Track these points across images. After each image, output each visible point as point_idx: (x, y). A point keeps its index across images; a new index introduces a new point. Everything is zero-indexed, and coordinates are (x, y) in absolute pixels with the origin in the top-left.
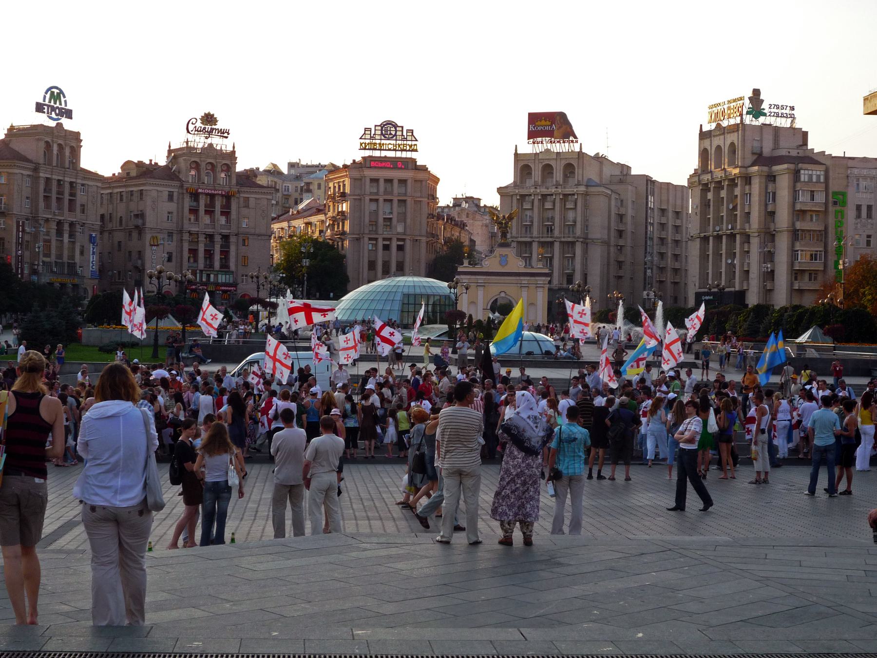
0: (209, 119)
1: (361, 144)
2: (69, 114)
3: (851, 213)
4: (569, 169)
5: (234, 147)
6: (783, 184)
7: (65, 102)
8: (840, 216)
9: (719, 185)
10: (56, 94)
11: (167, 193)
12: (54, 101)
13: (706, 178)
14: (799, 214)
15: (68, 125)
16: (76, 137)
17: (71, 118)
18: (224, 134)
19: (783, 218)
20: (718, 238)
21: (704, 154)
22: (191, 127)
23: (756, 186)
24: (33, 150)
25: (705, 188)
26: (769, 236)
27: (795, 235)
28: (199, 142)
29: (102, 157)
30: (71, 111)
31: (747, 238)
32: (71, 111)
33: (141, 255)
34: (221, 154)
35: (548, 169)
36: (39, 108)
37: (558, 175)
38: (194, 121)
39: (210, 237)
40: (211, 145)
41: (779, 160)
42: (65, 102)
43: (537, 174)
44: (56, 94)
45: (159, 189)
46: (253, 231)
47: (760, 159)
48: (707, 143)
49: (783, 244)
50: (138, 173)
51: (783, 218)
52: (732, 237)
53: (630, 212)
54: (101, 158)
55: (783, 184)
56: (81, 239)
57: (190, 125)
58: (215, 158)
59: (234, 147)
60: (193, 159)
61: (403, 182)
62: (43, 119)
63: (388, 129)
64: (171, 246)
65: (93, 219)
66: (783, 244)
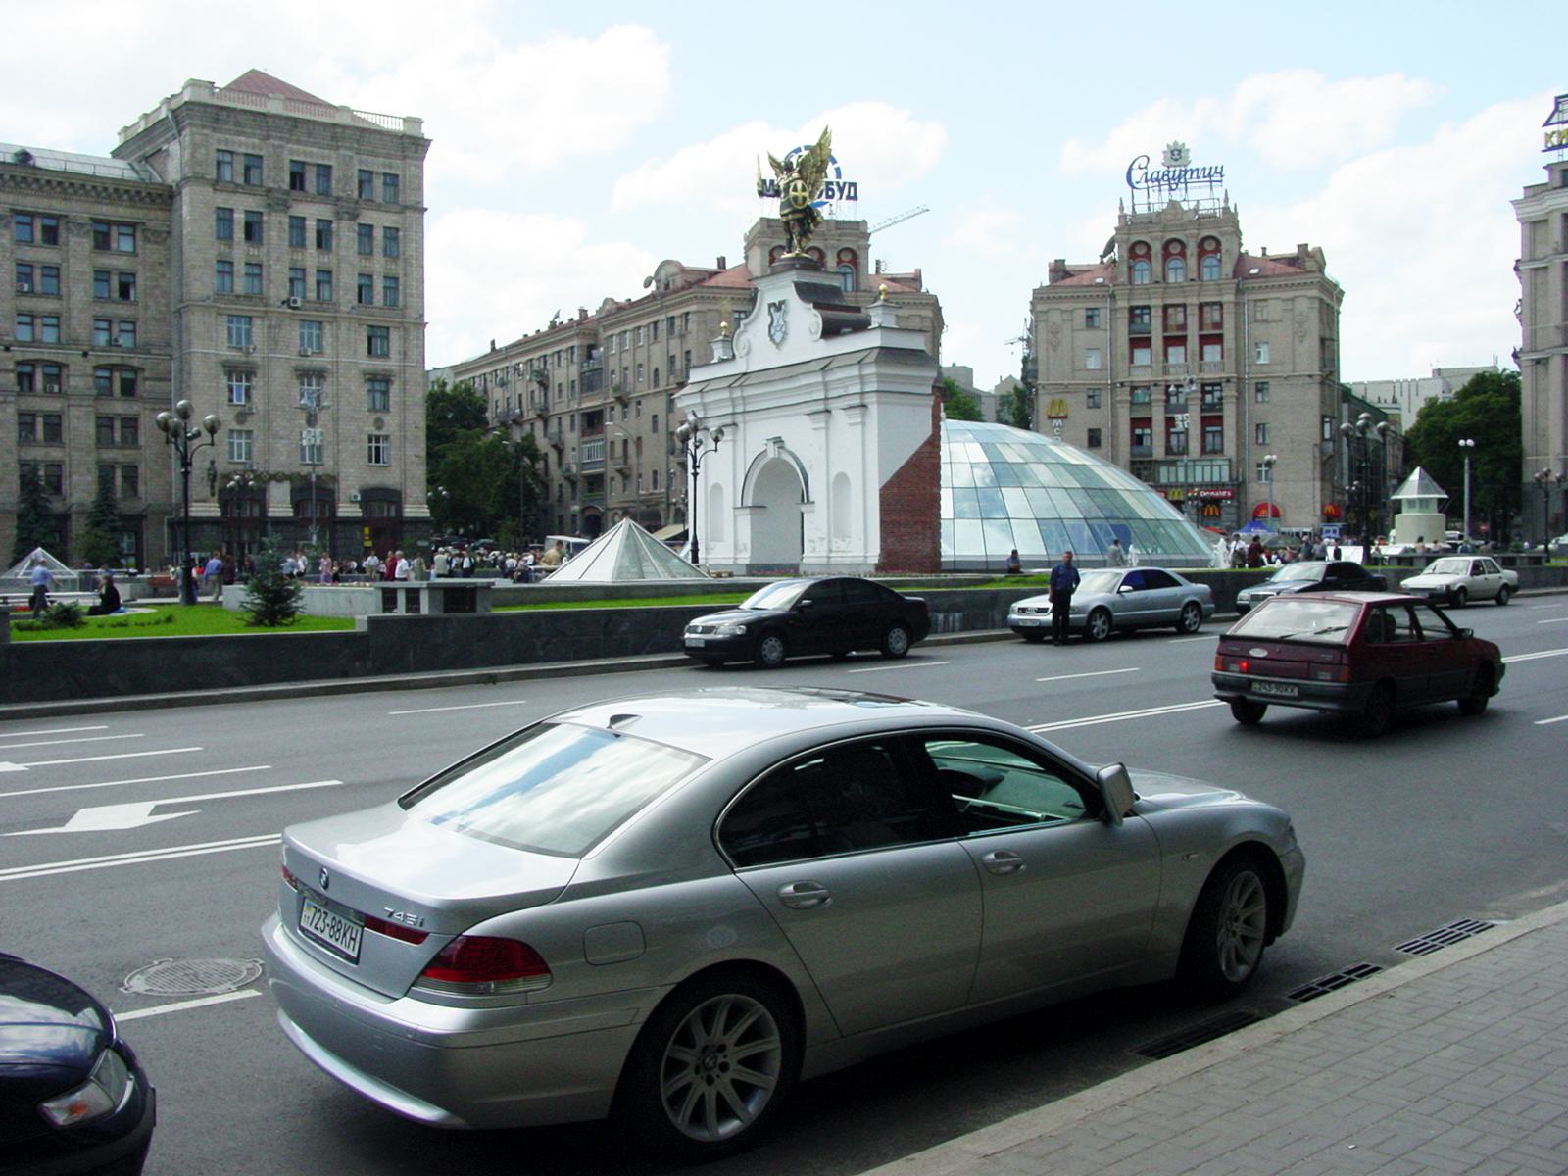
0: (1176, 153)
1: (1549, 137)
2: (850, 191)
5: (1226, 200)
7: (838, 170)
11: (1083, 313)
16: (858, 231)
17: (855, 198)
18: (1213, 176)
22: (1137, 175)
28: (1157, 200)
30: (854, 185)
32: (854, 185)
34: (1201, 220)
38: (1143, 162)
40: (1173, 204)
42: (838, 170)
45: (1063, 306)
46: (1277, 370)
57: (1133, 172)
58: (1183, 228)
59: (1226, 200)
60: (1135, 239)
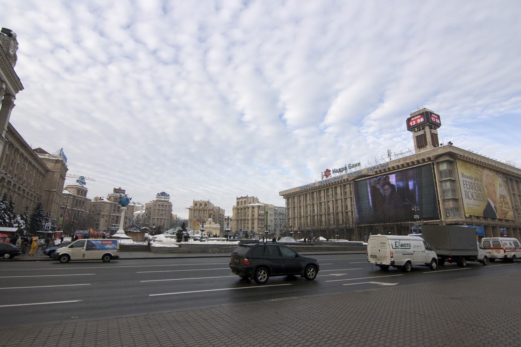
2: (85, 183)
3: (269, 215)
4: (206, 205)
8: (267, 216)
9: (242, 209)
12: (82, 180)
13: (238, 207)
14: (259, 215)
15: (84, 186)
19: (256, 216)
20: (241, 220)
21: (238, 203)
25: (238, 209)
27: (259, 219)
29: (91, 196)
31: (248, 220)
33: (98, 220)
35: (201, 205)
36: (78, 181)
37: (203, 206)
48: (238, 200)
49: (256, 222)
51: (256, 216)
52: (245, 220)
61: (166, 206)
63: (163, 194)
66: (256, 222)
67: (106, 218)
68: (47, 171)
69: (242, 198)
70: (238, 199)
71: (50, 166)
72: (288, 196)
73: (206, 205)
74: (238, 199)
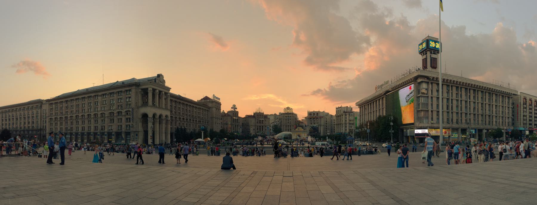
6: (348, 116)
10: (234, 106)
12: (234, 107)
14: (350, 120)
19: (348, 121)
23: (344, 116)
24: (231, 114)
26: (346, 124)
29: (242, 114)
37: (316, 115)
39: (260, 126)
41: (347, 112)
43: (312, 115)
44: (234, 106)
47: (344, 112)
49: (348, 125)
50: (248, 117)
51: (348, 121)
53: (328, 120)
54: (242, 114)
55: (348, 116)
56: (239, 127)
62: (233, 110)
63: (288, 108)
64: (254, 128)
65: (241, 124)
67: (254, 128)
68: (209, 108)
69: (339, 108)
70: (337, 108)
71: (210, 105)
72: (361, 105)
73: (317, 114)
74: (337, 108)
